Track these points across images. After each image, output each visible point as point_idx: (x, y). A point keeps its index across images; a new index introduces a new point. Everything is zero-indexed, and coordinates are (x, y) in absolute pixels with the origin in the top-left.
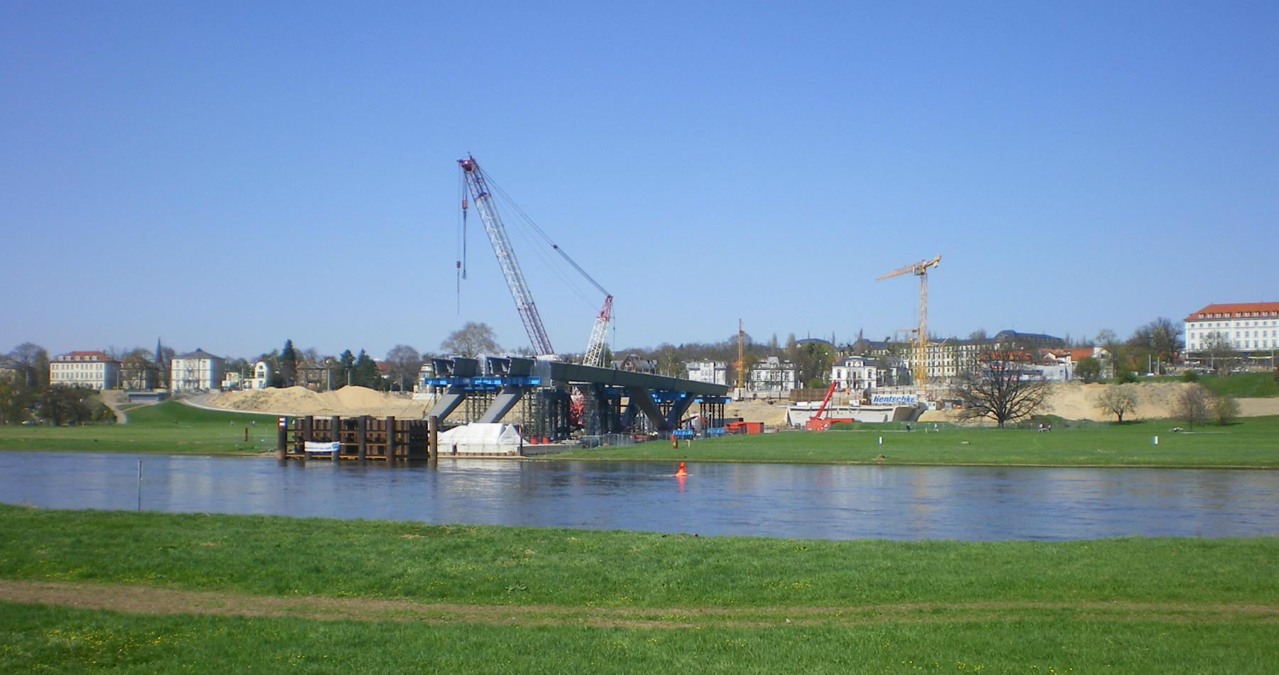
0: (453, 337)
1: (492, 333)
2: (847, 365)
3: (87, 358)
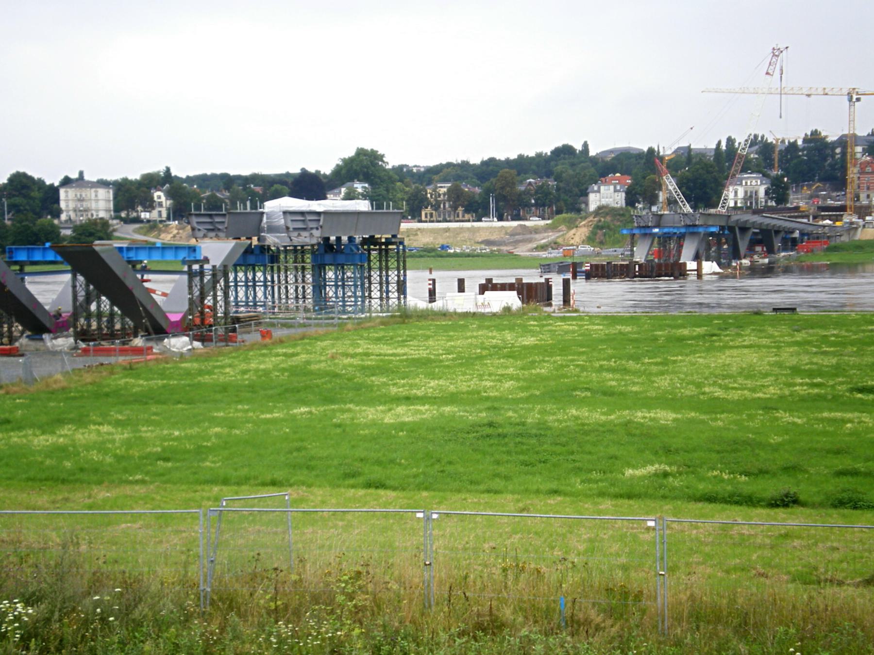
2: (744, 184)
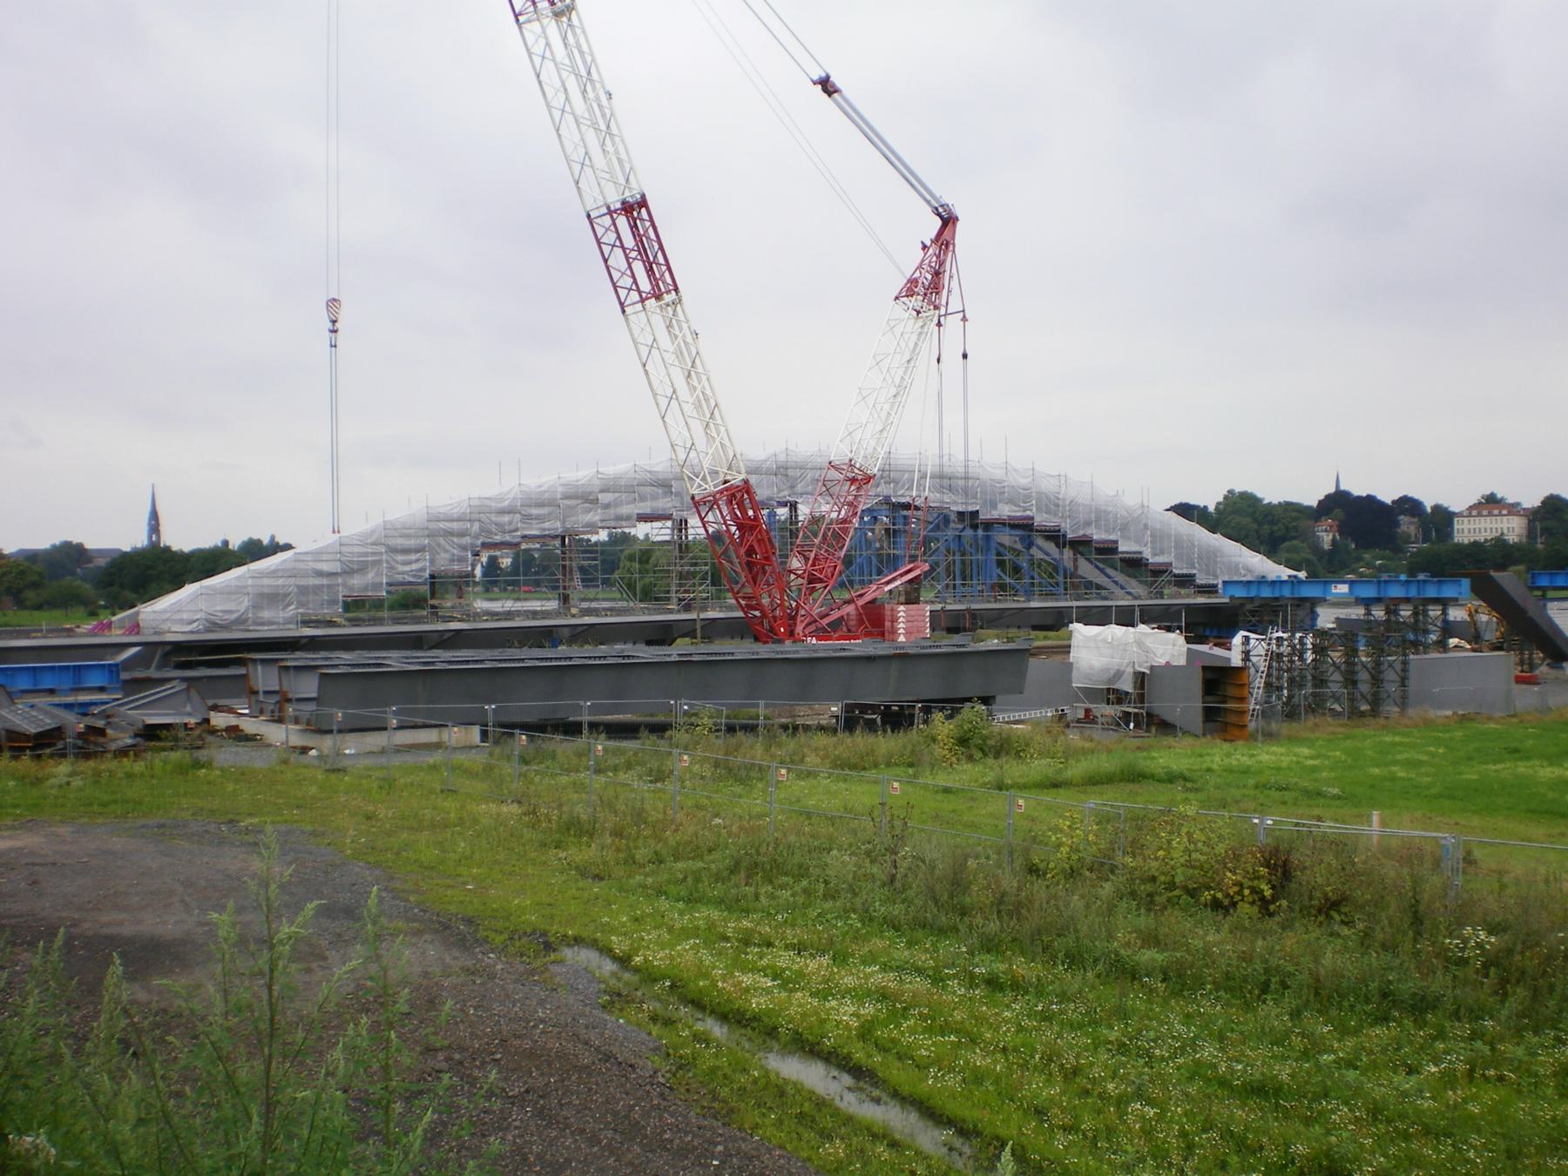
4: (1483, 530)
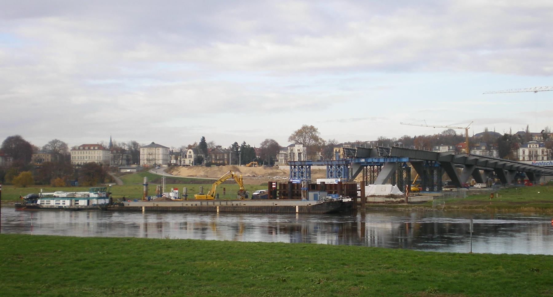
0: (295, 134)
1: (317, 132)
2: (529, 147)
3: (92, 148)
4: (85, 157)
